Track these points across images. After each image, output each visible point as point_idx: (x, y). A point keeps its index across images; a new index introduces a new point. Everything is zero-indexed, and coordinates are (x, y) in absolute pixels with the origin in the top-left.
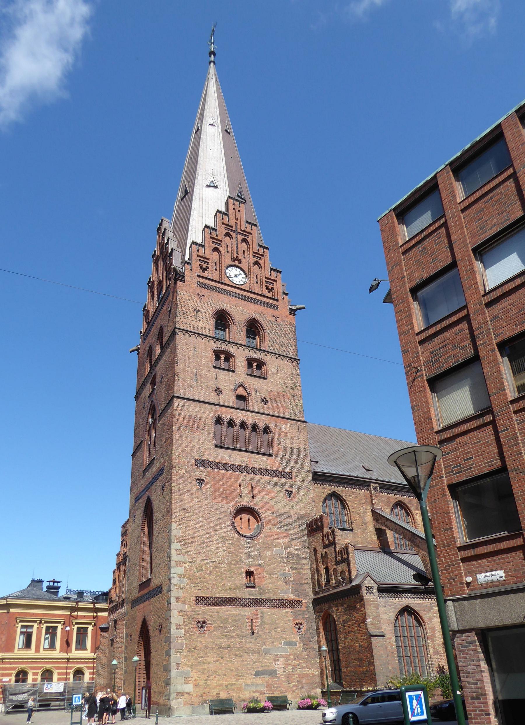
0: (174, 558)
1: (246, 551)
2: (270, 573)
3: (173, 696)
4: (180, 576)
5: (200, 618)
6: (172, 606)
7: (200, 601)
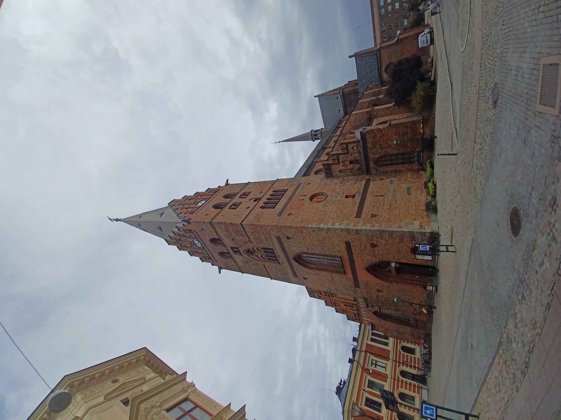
0: (329, 226)
1: (334, 198)
2: (349, 189)
3: (422, 231)
4: (340, 224)
5: (369, 216)
6: (359, 228)
7: (359, 215)
